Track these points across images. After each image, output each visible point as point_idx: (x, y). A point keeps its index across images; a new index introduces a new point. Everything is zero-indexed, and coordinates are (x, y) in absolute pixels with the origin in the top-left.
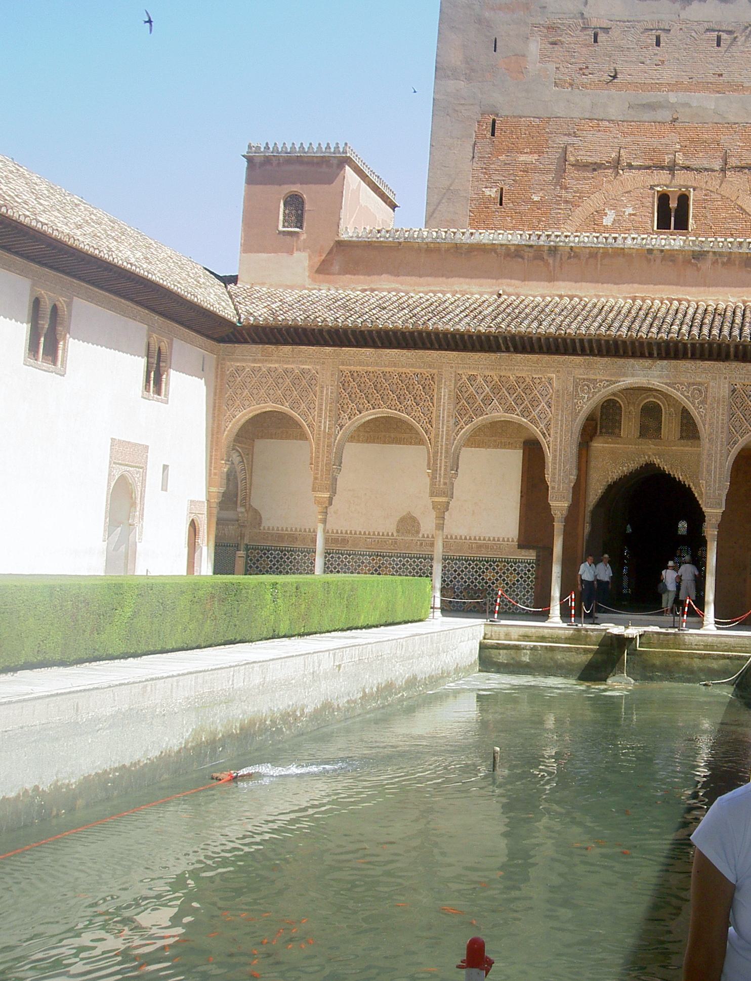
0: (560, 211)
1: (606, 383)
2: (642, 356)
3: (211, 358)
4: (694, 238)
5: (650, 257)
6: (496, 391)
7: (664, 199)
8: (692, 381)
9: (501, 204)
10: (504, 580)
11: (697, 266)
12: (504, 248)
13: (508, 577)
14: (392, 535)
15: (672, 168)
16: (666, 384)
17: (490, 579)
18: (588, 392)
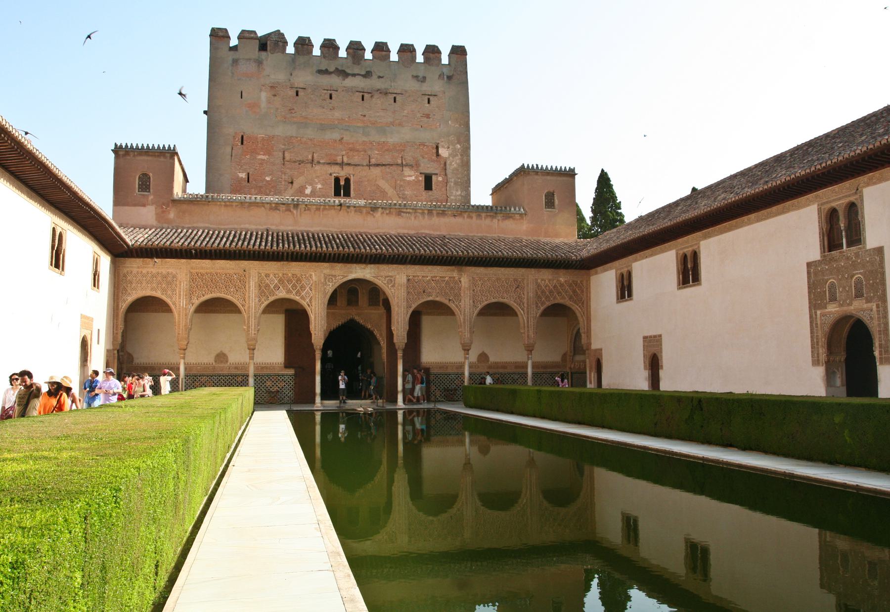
0: (282, 186)
1: (342, 277)
6: (281, 282)
7: (337, 180)
8: (387, 275)
9: (248, 182)
10: (277, 386)
11: (373, 215)
12: (268, 205)
13: (279, 384)
14: (212, 364)
15: (342, 165)
16: (373, 277)
17: (269, 385)
18: (332, 282)
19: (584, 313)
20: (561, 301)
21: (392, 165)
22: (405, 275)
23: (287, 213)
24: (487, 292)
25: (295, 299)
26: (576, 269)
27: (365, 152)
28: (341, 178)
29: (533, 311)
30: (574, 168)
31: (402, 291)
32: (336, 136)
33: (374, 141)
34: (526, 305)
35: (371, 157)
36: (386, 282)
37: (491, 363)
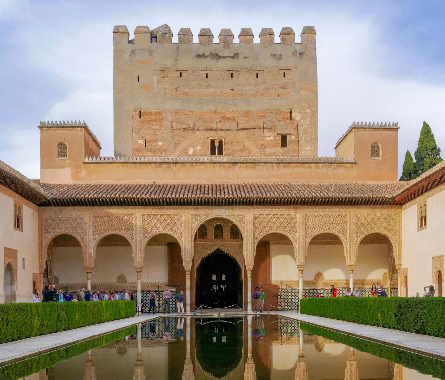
5: (215, 165)
7: (213, 142)
21: (255, 128)
22: (253, 213)
24: (317, 225)
25: (170, 234)
27: (234, 119)
28: (215, 140)
30: (397, 123)
31: (251, 226)
32: (212, 108)
33: (240, 110)
35: (239, 123)
36: (238, 220)
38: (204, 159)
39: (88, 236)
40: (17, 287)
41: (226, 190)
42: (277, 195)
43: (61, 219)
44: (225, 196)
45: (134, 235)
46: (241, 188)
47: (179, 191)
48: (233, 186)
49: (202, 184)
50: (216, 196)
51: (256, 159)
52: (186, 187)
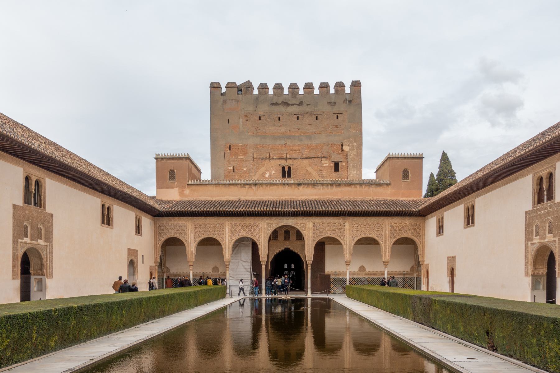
2: (286, 216)
3: (152, 222)
4: (297, 180)
18: (271, 227)
19: (420, 243)
20: (407, 236)
23: (250, 188)
25: (251, 237)
26: (416, 216)
29: (388, 242)
31: (310, 232)
34: (384, 238)
37: (367, 272)
38: (276, 181)
39: (190, 239)
40: (137, 277)
41: (292, 204)
42: (330, 209)
43: (170, 226)
44: (291, 209)
45: (224, 238)
46: (303, 203)
47: (257, 206)
48: (298, 202)
49: (274, 200)
50: (284, 210)
51: (312, 181)
52: (263, 202)
